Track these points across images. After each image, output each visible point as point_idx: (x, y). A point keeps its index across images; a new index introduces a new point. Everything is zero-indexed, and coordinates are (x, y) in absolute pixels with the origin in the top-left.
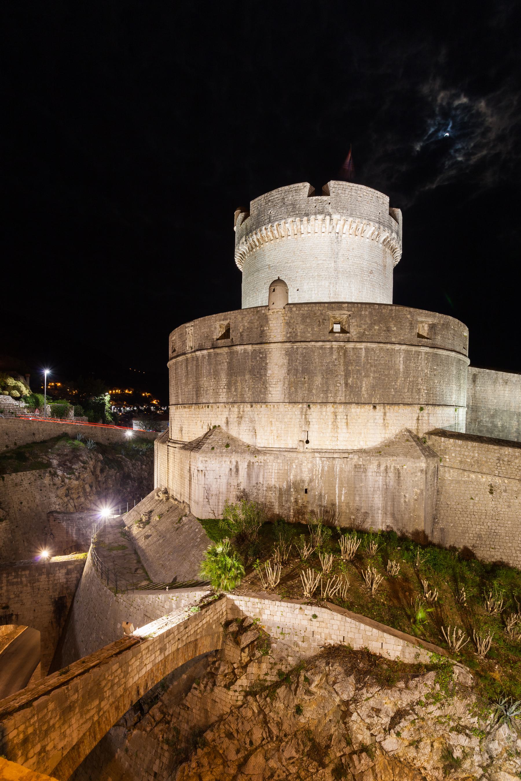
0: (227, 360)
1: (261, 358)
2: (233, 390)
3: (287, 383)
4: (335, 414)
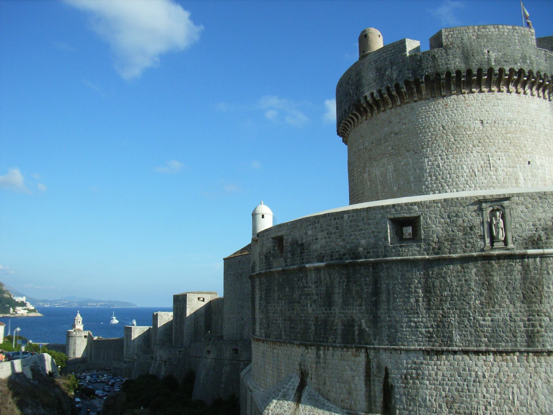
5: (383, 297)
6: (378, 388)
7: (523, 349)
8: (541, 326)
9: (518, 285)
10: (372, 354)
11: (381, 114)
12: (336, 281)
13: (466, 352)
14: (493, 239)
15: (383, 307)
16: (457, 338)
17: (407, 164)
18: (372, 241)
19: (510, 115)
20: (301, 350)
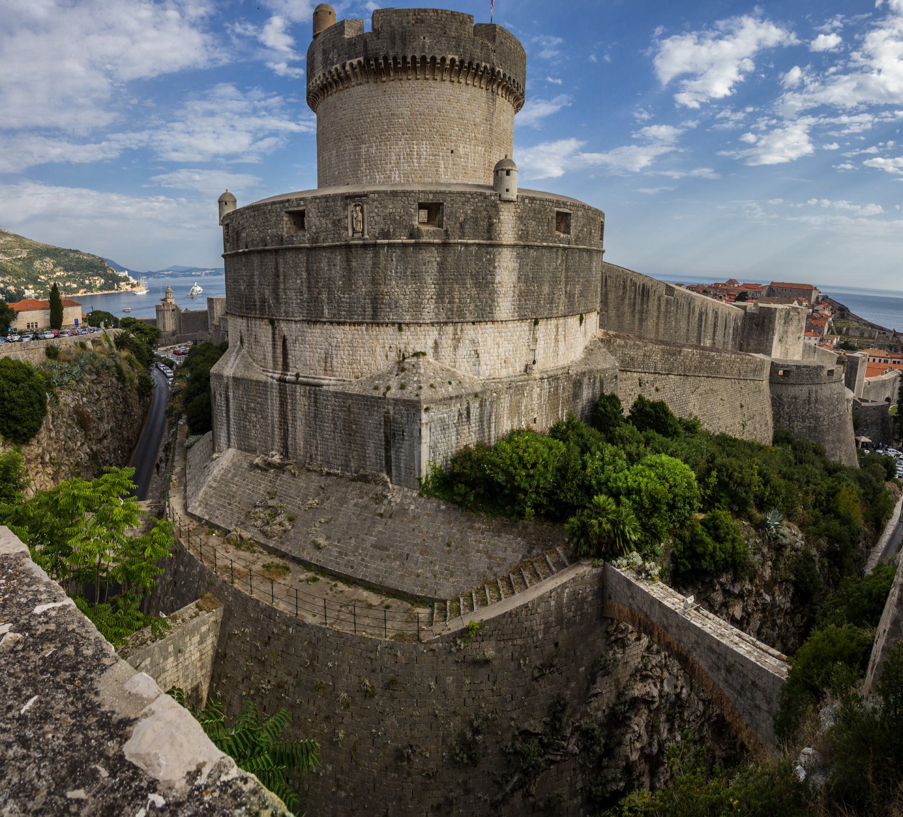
0: (438, 259)
1: (489, 260)
2: (447, 301)
3: (517, 292)
6: (279, 351)
7: (368, 321)
8: (382, 303)
9: (369, 269)
11: (330, 97)
13: (331, 323)
16: (326, 311)
17: (345, 150)
20: (240, 320)
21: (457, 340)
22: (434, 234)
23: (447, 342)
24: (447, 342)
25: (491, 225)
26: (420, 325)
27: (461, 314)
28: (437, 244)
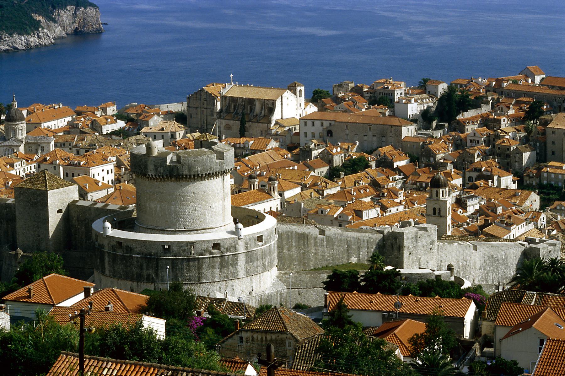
4: (260, 277)
5: (160, 268)
9: (196, 266)
10: (156, 284)
12: (144, 262)
14: (191, 253)
15: (160, 271)
18: (156, 251)
19: (204, 189)
20: (131, 282)
21: (226, 286)
22: (219, 253)
23: (223, 287)
24: (223, 287)
25: (236, 247)
26: (214, 282)
27: (227, 277)
28: (219, 257)
